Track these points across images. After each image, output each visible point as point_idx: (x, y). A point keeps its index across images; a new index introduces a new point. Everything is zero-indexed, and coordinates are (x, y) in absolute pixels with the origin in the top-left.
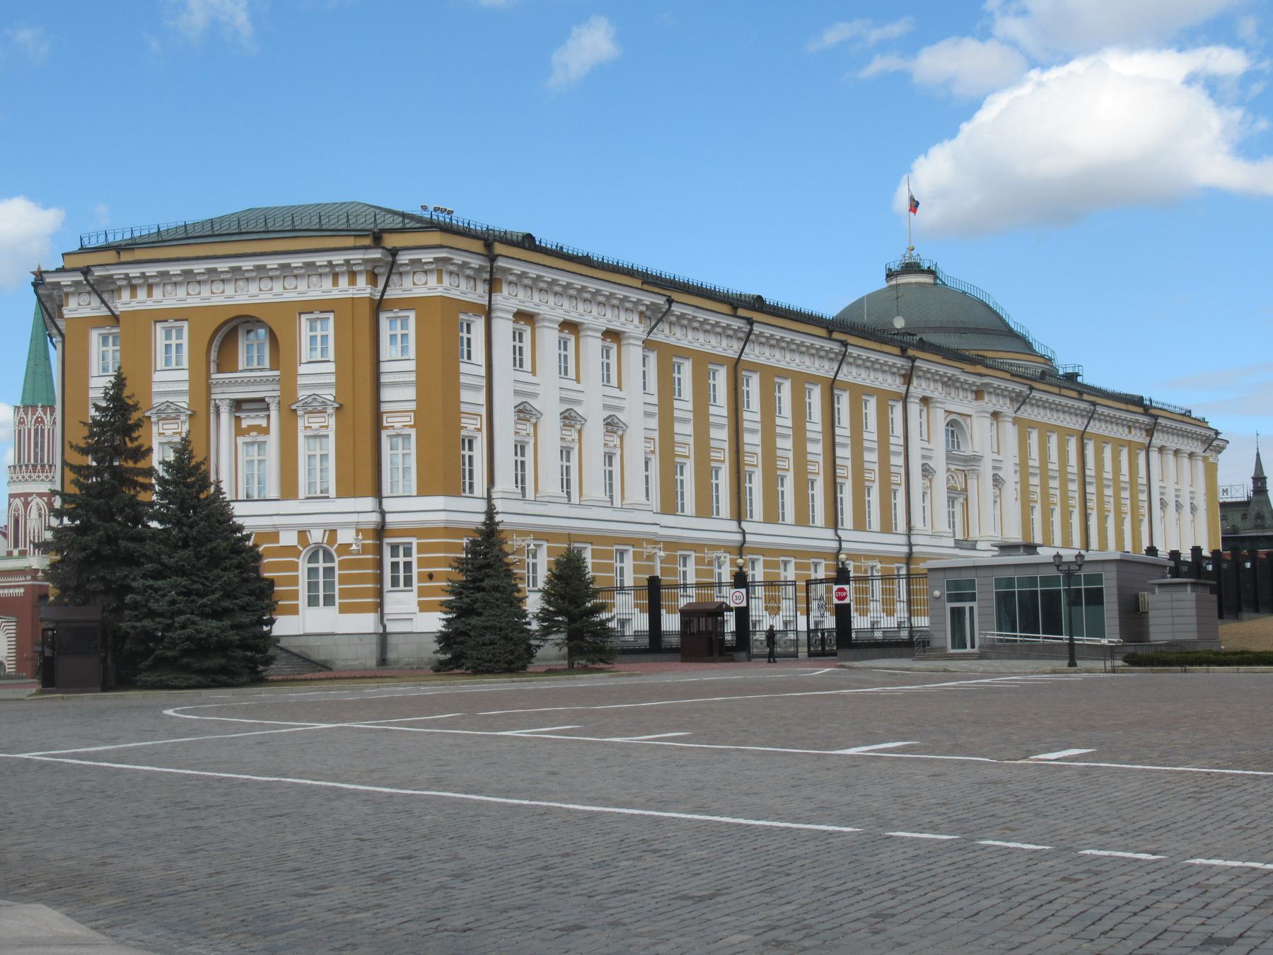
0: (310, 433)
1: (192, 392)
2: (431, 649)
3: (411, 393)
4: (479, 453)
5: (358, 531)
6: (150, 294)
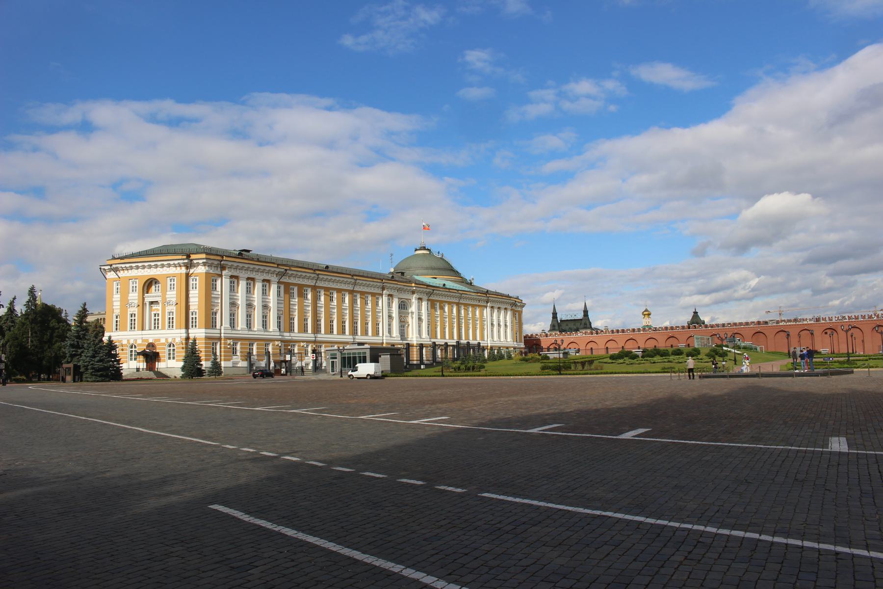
2: (179, 373)
3: (197, 299)
4: (218, 316)
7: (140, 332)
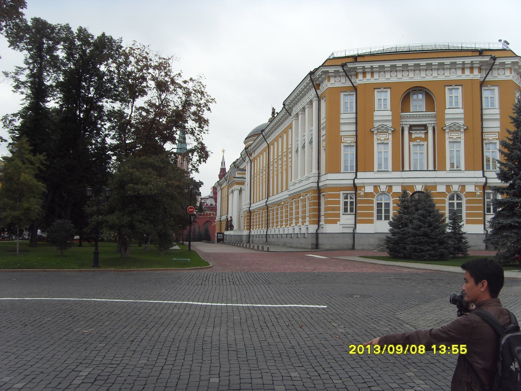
0: (451, 140)
1: (393, 121)
3: (497, 124)
5: (476, 186)
6: (372, 76)
7: (398, 174)
